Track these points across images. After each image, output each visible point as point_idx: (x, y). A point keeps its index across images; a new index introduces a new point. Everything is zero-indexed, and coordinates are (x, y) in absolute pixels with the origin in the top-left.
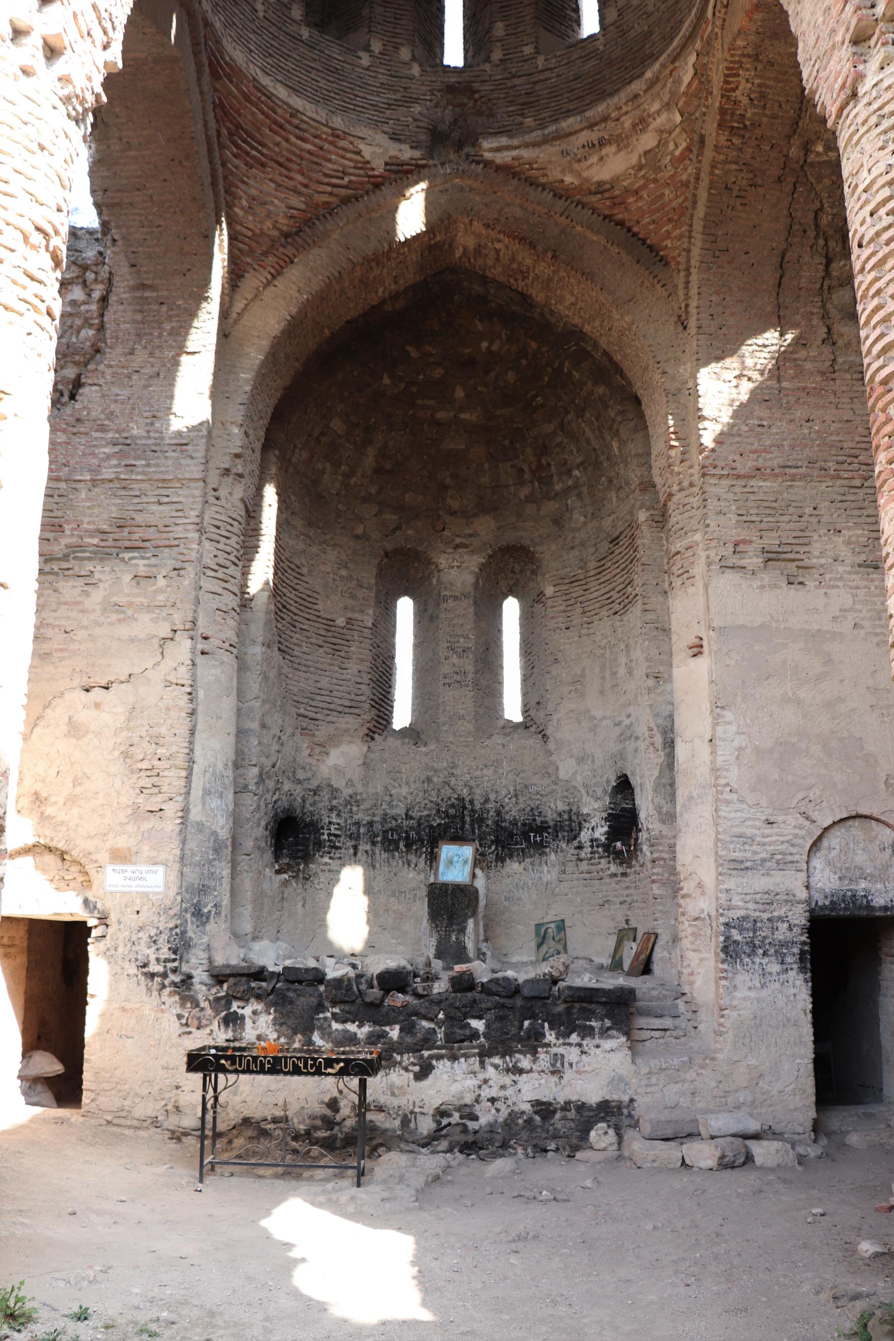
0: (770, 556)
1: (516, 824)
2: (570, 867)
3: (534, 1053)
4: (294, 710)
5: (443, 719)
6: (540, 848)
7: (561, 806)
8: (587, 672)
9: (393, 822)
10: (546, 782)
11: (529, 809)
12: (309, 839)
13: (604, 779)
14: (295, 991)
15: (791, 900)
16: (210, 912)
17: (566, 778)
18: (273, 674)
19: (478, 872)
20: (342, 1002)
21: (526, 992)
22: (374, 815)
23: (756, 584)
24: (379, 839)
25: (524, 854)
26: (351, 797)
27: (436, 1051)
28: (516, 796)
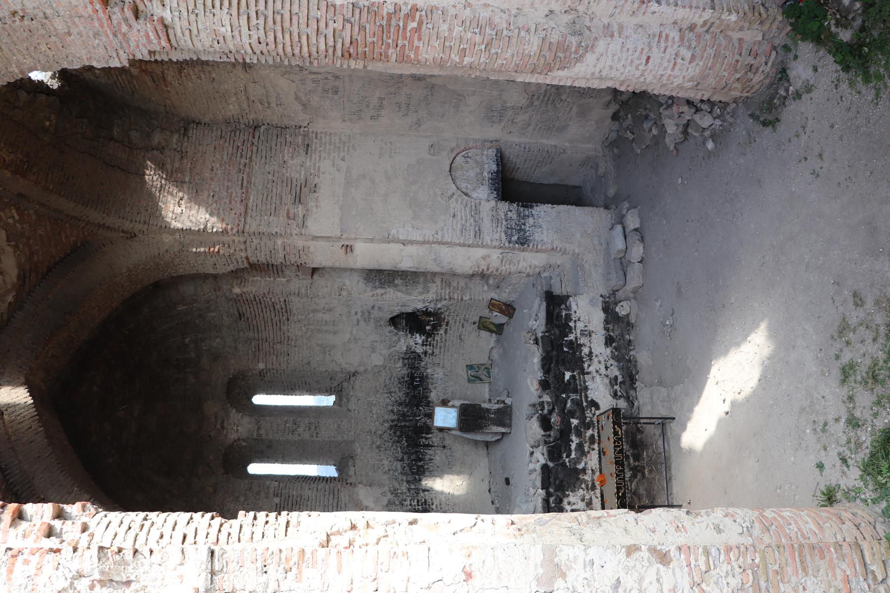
0: (297, 200)
2: (436, 360)
3: (581, 345)
5: (339, 438)
6: (423, 379)
7: (400, 364)
8: (320, 342)
10: (383, 373)
13: (388, 334)
15: (495, 209)
19: (450, 404)
22: (402, 480)
23: (315, 210)
25: (426, 389)
28: (391, 393)
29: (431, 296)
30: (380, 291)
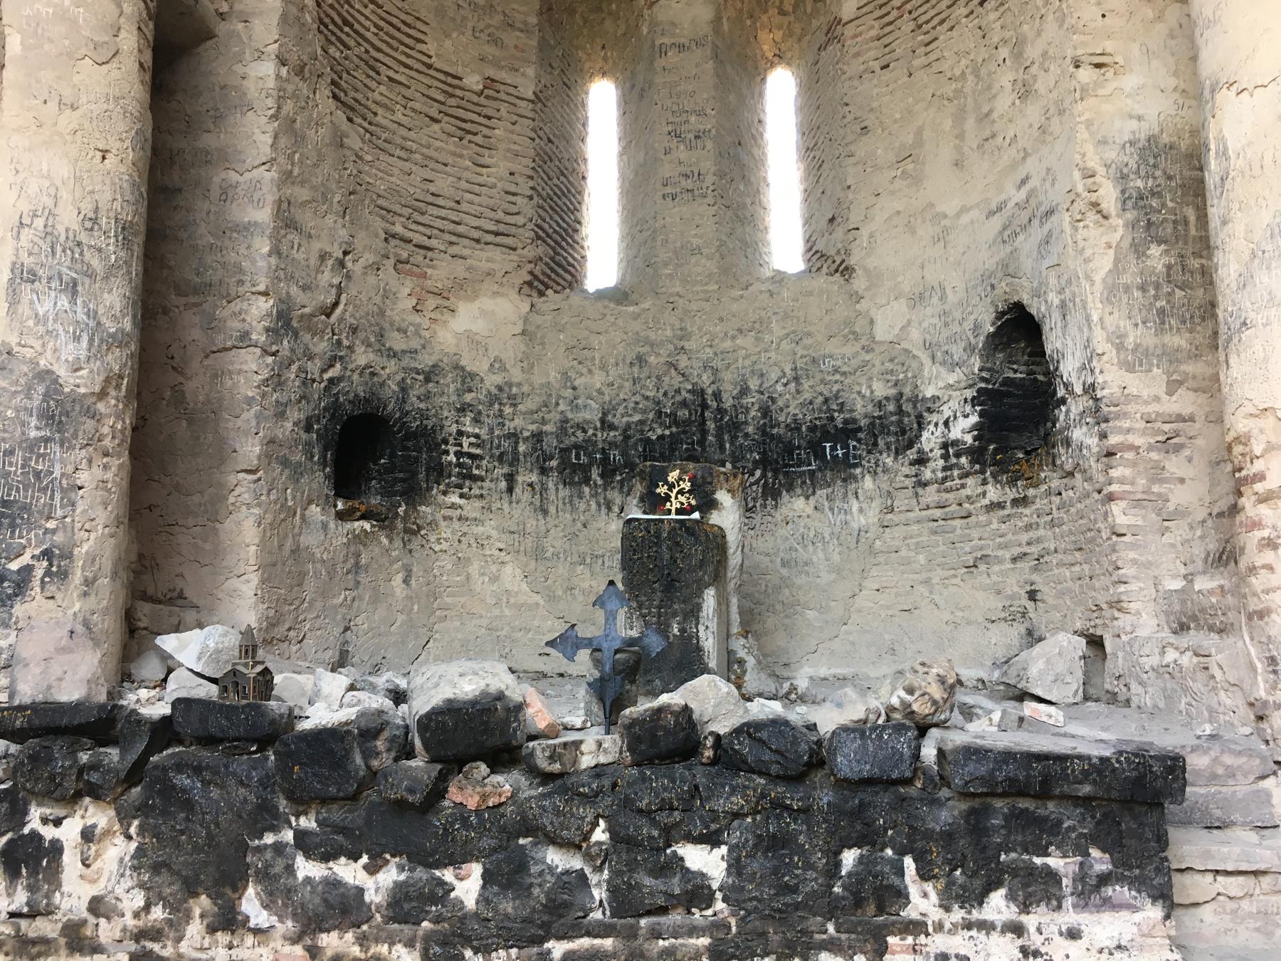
1: (798, 429)
4: (379, 224)
6: (844, 469)
7: (881, 390)
8: (927, 134)
9: (579, 433)
10: (849, 350)
11: (821, 399)
12: (417, 460)
13: (968, 325)
14: (198, 770)
16: (28, 569)
17: (889, 338)
18: (317, 136)
20: (325, 801)
21: (847, 763)
22: (544, 422)
24: (554, 463)
25: (814, 482)
26: (500, 389)
27: (584, 943)
28: (796, 379)
29: (1112, 380)
30: (1109, 195)
